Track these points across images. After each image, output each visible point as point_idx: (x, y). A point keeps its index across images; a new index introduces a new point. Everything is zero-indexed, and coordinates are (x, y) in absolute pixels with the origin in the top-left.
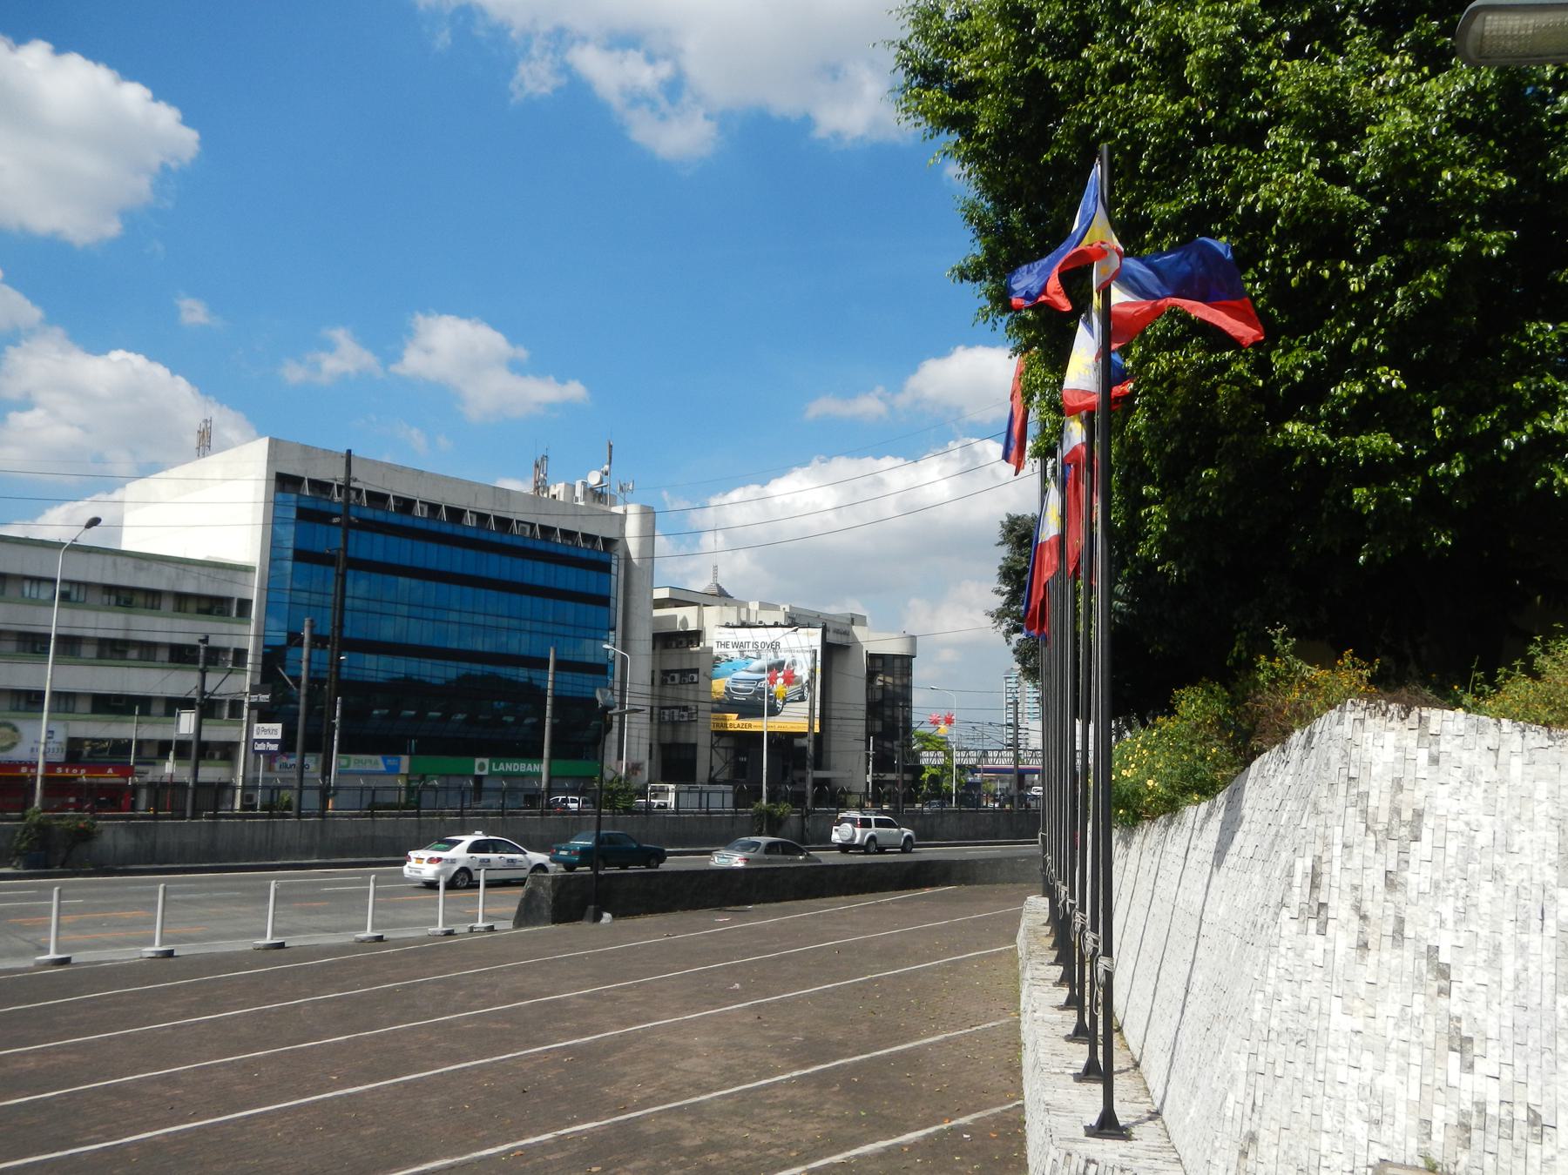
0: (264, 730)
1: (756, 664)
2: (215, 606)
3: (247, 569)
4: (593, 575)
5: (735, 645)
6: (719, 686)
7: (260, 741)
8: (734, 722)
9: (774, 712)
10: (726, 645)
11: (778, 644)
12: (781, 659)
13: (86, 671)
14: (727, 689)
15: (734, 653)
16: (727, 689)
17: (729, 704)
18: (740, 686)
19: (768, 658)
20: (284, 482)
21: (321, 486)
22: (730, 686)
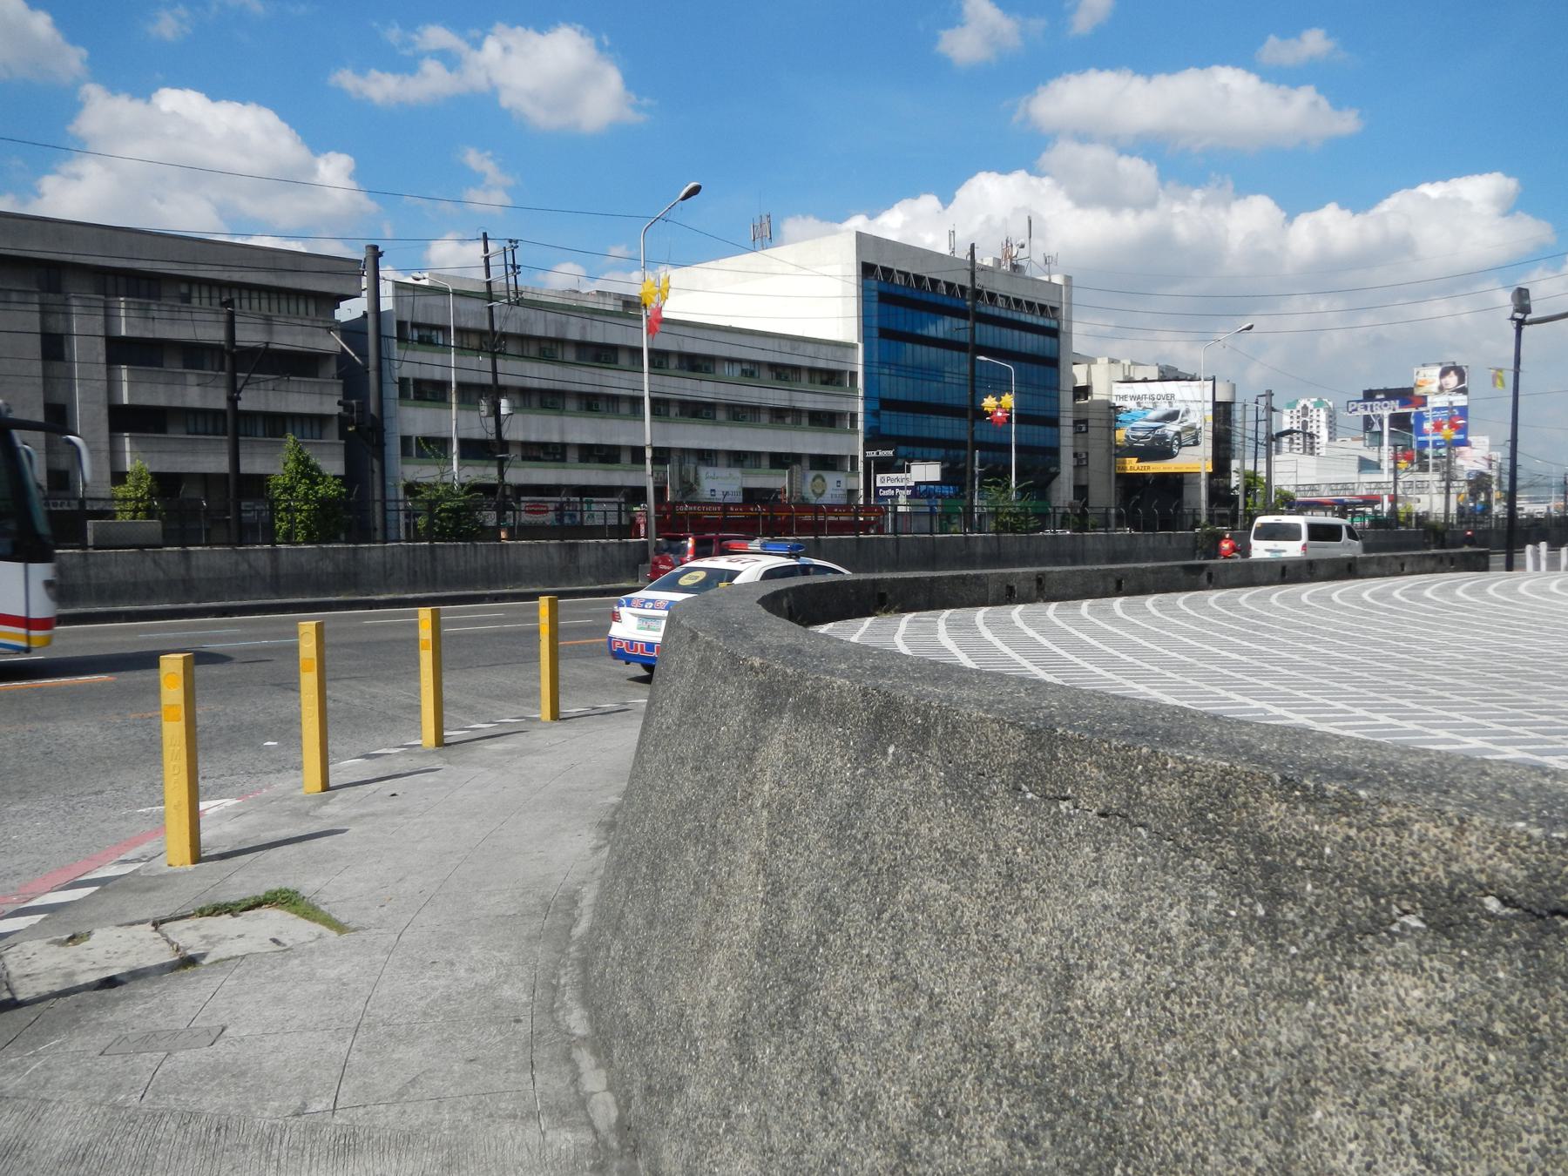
0: (892, 480)
1: (1153, 415)
2: (832, 378)
3: (850, 346)
4: (1048, 339)
5: (1133, 397)
6: (1120, 435)
7: (885, 488)
8: (1133, 465)
9: (1168, 454)
10: (1124, 397)
11: (1173, 396)
12: (1175, 408)
13: (725, 431)
14: (1127, 436)
15: (1131, 404)
16: (1127, 436)
17: (1132, 450)
18: (1139, 434)
19: (1164, 408)
20: (867, 270)
21: (887, 272)
22: (1131, 433)
